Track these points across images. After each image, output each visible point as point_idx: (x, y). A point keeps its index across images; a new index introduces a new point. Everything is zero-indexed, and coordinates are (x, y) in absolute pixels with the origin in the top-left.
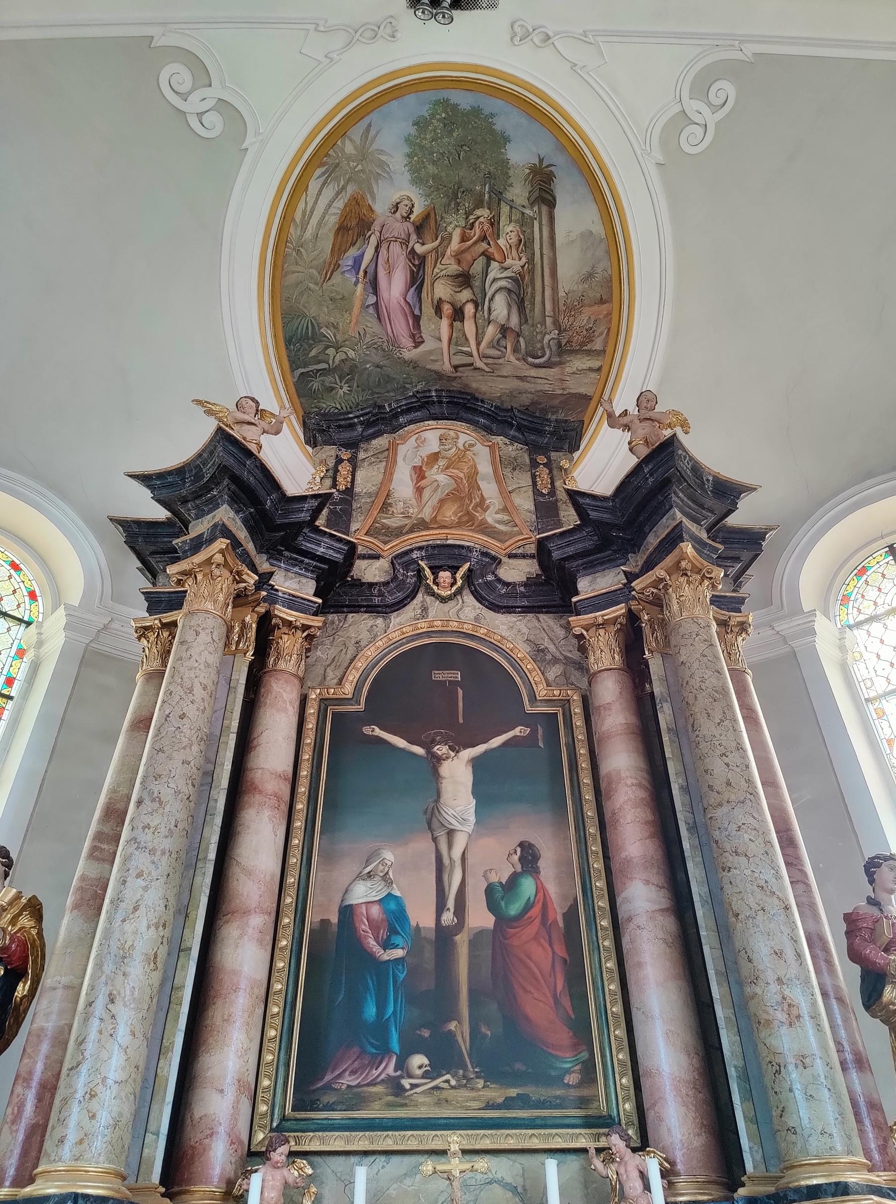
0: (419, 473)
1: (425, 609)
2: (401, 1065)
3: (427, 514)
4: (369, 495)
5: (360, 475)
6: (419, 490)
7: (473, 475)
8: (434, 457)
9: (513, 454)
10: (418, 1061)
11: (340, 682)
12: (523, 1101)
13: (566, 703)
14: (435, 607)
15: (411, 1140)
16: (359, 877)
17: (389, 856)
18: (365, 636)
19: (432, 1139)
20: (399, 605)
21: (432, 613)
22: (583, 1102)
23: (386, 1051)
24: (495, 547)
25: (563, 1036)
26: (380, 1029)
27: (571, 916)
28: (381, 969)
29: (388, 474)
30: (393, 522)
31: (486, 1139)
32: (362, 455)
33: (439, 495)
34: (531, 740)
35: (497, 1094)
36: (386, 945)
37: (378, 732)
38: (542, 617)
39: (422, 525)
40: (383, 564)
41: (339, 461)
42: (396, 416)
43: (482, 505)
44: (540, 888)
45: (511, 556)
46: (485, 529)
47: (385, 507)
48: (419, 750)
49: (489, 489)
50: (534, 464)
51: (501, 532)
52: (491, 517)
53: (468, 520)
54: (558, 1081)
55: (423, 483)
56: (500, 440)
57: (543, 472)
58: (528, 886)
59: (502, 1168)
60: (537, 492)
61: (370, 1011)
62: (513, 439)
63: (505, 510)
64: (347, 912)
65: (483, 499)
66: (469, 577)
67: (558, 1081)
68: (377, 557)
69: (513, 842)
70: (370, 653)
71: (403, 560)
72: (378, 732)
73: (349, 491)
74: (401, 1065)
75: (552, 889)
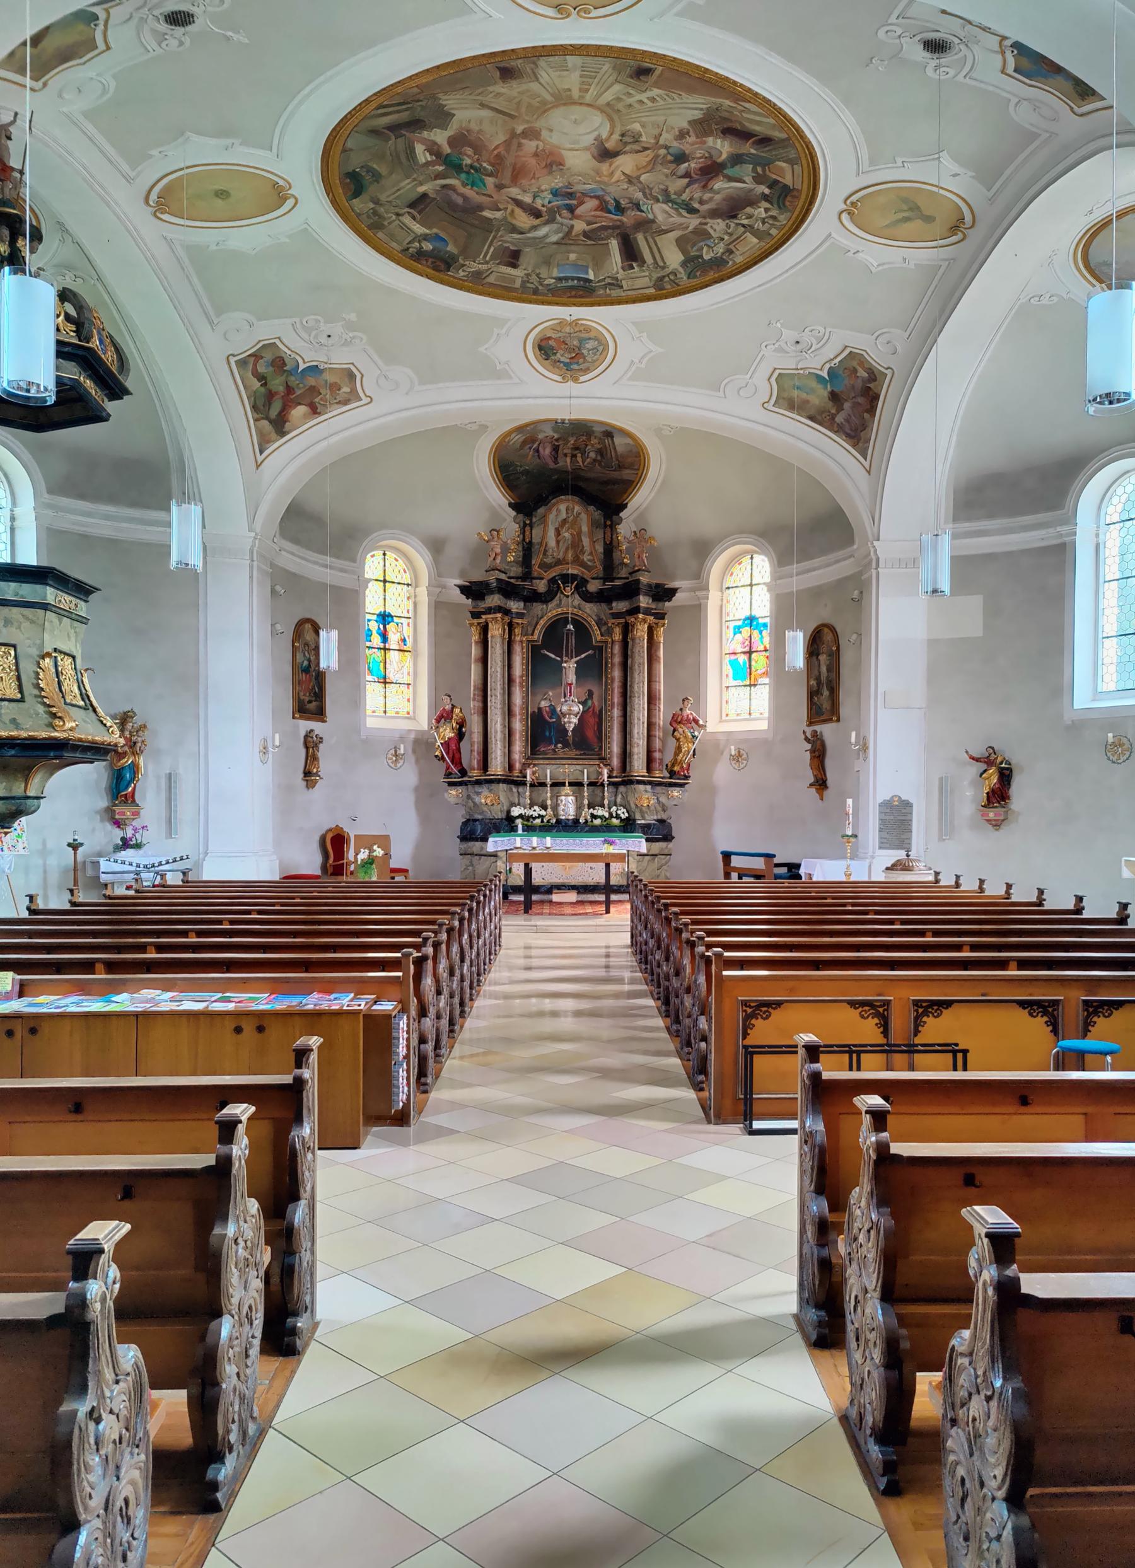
0: (558, 532)
1: (560, 601)
2: (555, 746)
3: (561, 556)
4: (538, 544)
5: (534, 531)
6: (558, 542)
7: (580, 533)
8: (564, 521)
9: (597, 517)
10: (560, 745)
11: (532, 634)
12: (584, 754)
13: (606, 642)
14: (564, 600)
15: (558, 762)
16: (542, 699)
17: (551, 694)
18: (540, 613)
19: (564, 762)
20: (552, 599)
21: (563, 602)
22: (598, 755)
23: (551, 744)
24: (587, 575)
25: (596, 740)
26: (551, 738)
27: (601, 711)
28: (549, 723)
29: (545, 531)
30: (549, 560)
31: (575, 762)
32: (534, 520)
33: (566, 545)
34: (593, 655)
35: (578, 752)
36: (551, 718)
37: (546, 652)
38: (603, 604)
39: (559, 562)
40: (544, 582)
41: (525, 525)
42: (547, 497)
43: (583, 552)
44: (593, 703)
45: (593, 578)
46: (583, 564)
47: (545, 551)
48: (558, 659)
49: (586, 541)
50: (605, 526)
51: (590, 566)
52: (586, 558)
53: (577, 561)
54: (593, 750)
55: (560, 538)
56: (591, 508)
57: (608, 530)
58: (590, 703)
59: (578, 767)
60: (605, 543)
61: (547, 734)
62: (598, 509)
63: (591, 554)
64: (540, 709)
65: (583, 547)
66: (577, 588)
67: (593, 750)
68: (542, 579)
69: (586, 689)
70: (542, 622)
71: (552, 581)
72: (546, 652)
73: (530, 543)
74: (555, 746)
75: (596, 704)
